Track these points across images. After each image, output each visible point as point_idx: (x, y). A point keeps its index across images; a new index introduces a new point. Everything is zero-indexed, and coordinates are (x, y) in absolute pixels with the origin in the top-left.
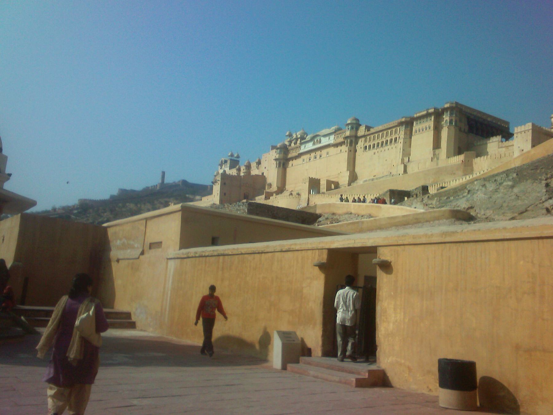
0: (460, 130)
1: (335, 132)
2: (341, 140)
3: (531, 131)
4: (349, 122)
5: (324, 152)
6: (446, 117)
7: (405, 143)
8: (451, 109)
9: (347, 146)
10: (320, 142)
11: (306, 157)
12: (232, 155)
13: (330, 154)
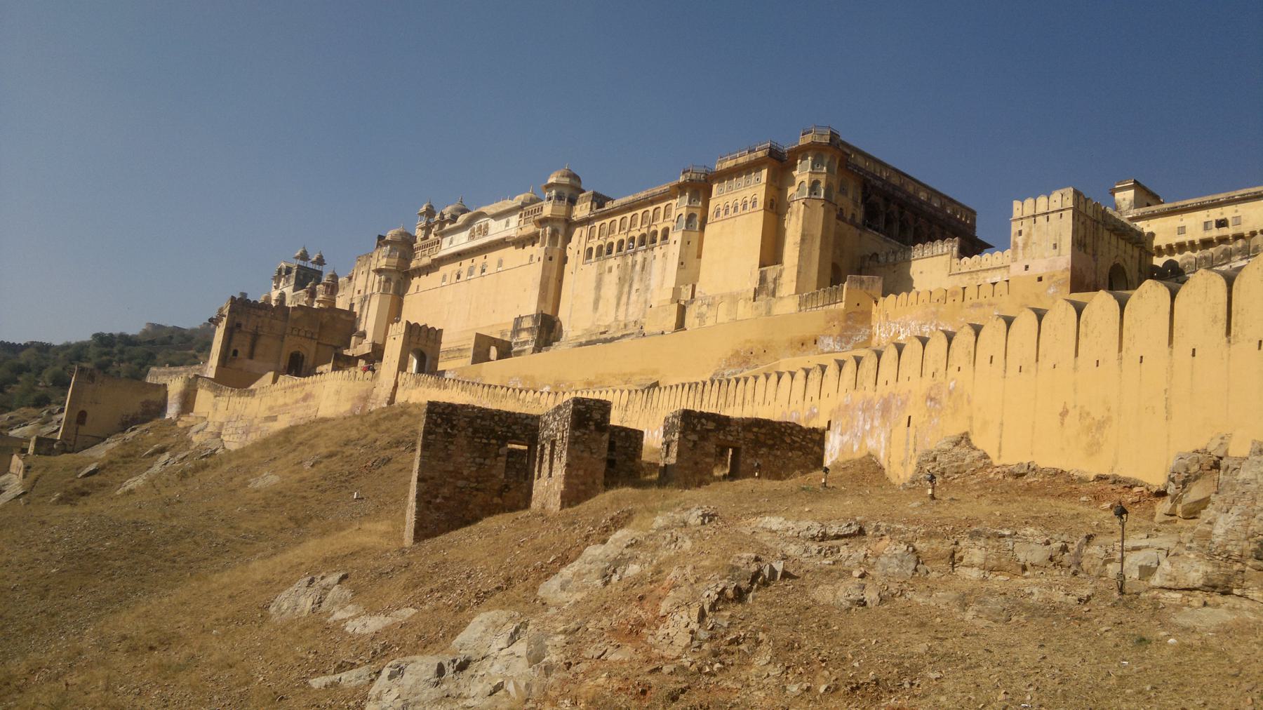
0: (840, 217)
1: (521, 208)
2: (530, 229)
3: (1068, 215)
4: (552, 180)
5: (493, 256)
6: (802, 174)
7: (686, 243)
8: (815, 150)
9: (543, 245)
10: (486, 233)
11: (448, 269)
12: (304, 256)
13: (506, 265)
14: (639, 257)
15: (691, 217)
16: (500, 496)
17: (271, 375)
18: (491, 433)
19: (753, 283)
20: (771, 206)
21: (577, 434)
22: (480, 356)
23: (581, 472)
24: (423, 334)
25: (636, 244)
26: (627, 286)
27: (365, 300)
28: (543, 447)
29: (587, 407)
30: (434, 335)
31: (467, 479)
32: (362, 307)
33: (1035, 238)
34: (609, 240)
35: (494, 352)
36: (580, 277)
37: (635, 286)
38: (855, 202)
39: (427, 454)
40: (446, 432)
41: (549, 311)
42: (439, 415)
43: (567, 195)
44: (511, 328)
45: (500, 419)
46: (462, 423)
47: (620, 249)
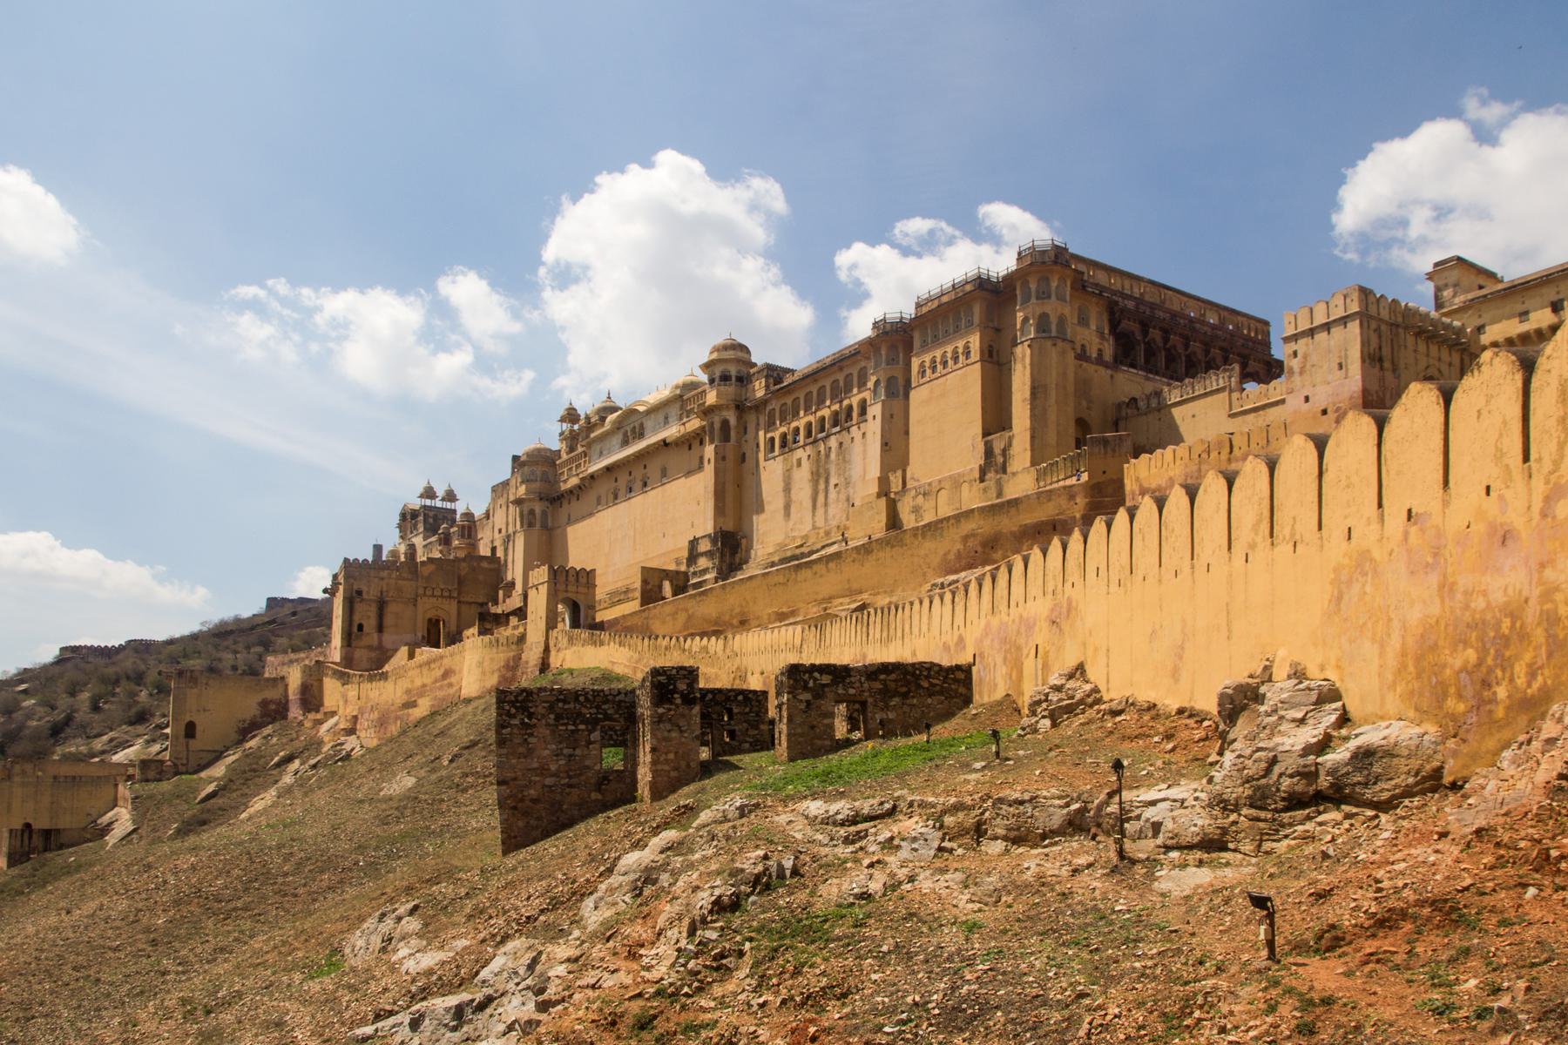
7: (888, 418)
11: (603, 488)
12: (429, 493)
14: (833, 442)
15: (891, 382)
16: (599, 790)
18: (577, 717)
19: (977, 460)
20: (991, 355)
21: (661, 710)
23: (671, 756)
24: (571, 579)
26: (822, 482)
27: (508, 539)
29: (670, 678)
31: (555, 775)
32: (506, 550)
33: (1314, 358)
34: (794, 424)
35: (667, 588)
37: (833, 481)
39: (504, 751)
40: (523, 723)
41: (729, 526)
42: (513, 703)
44: (686, 554)
45: (587, 699)
46: (541, 710)
47: (809, 434)
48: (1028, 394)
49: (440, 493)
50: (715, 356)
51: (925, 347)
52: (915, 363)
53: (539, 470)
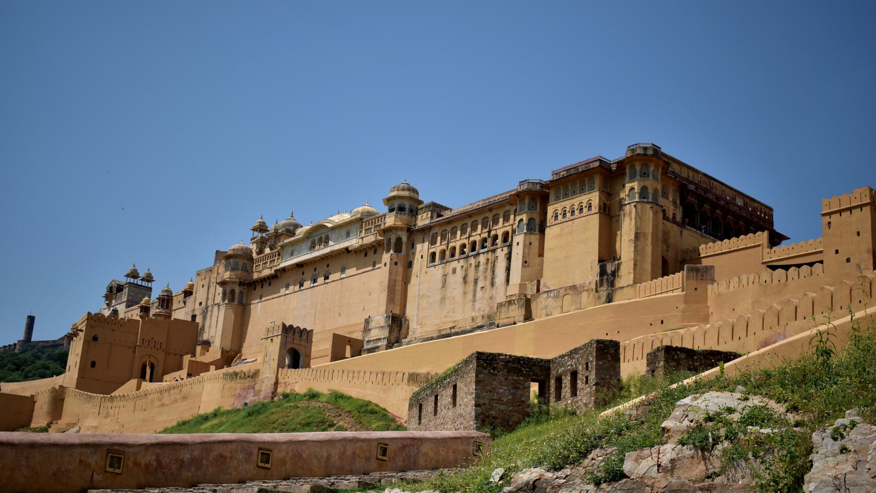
12: (134, 274)
17: (133, 382)
21: (600, 363)
22: (337, 355)
25: (477, 247)
28: (559, 380)
30: (306, 335)
36: (425, 278)
37: (480, 284)
38: (674, 203)
39: (479, 387)
41: (397, 311)
43: (407, 206)
47: (462, 252)
48: (633, 237)
49: (142, 274)
50: (394, 193)
51: (557, 199)
52: (550, 210)
53: (241, 262)
